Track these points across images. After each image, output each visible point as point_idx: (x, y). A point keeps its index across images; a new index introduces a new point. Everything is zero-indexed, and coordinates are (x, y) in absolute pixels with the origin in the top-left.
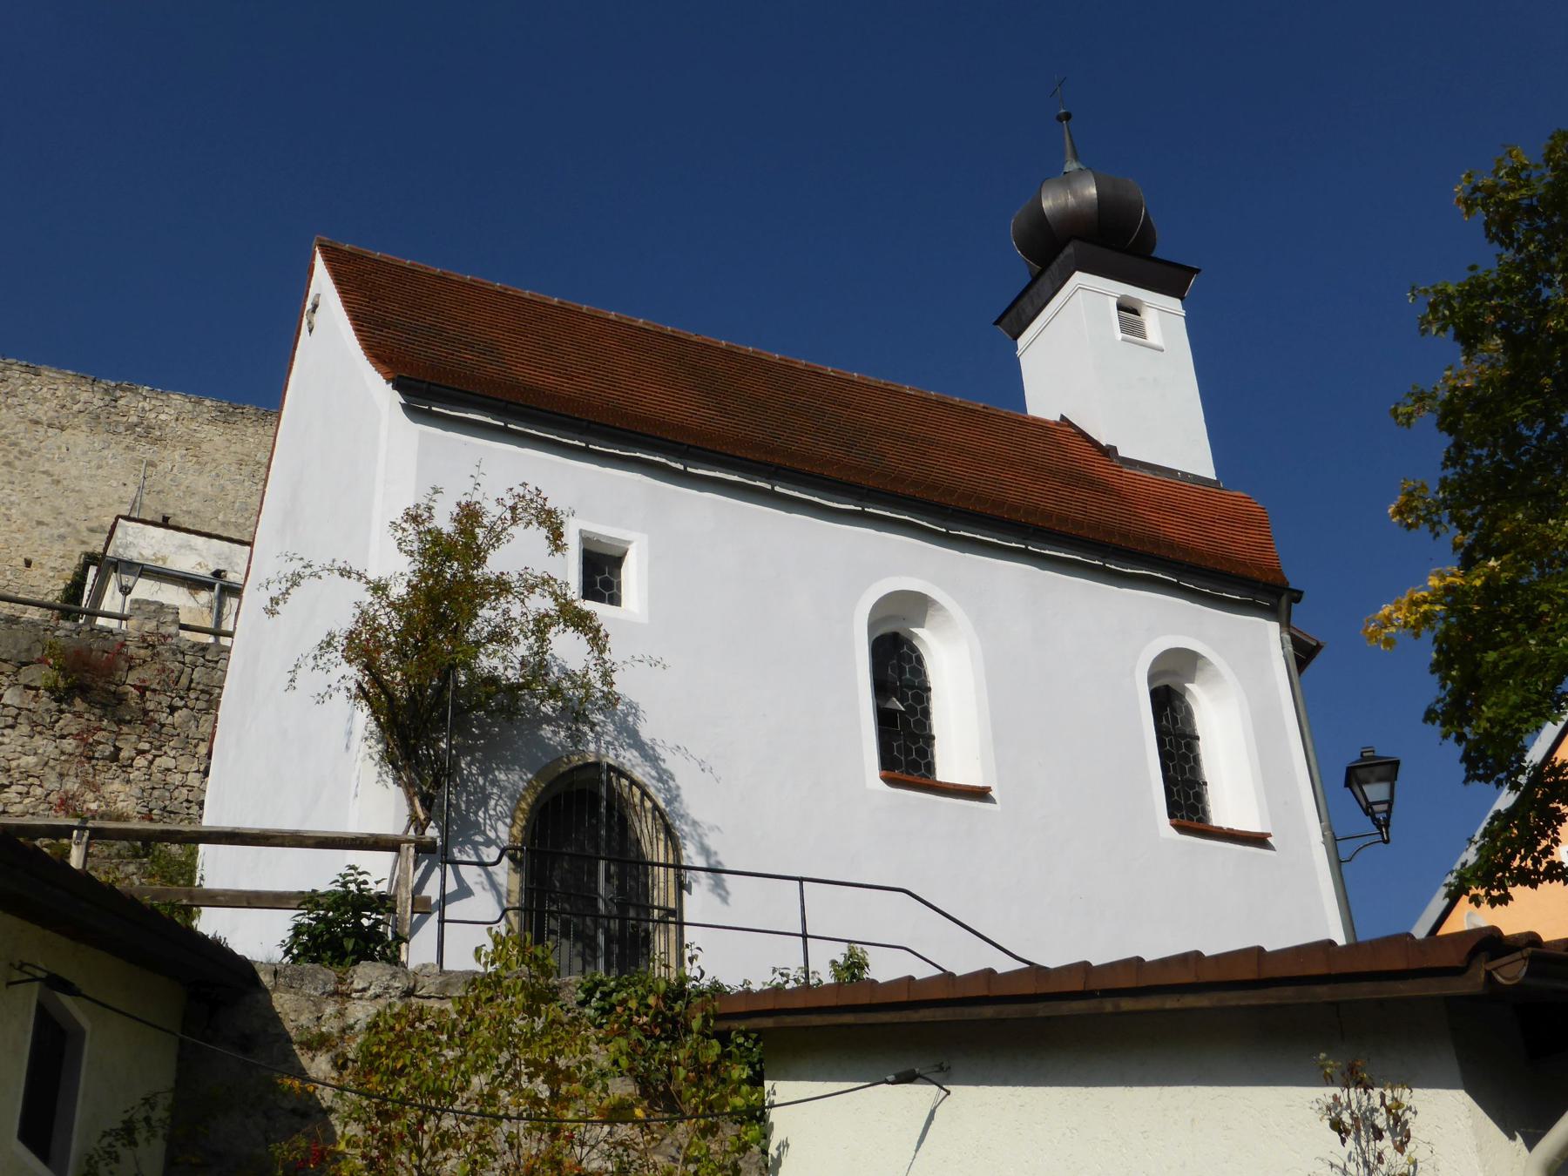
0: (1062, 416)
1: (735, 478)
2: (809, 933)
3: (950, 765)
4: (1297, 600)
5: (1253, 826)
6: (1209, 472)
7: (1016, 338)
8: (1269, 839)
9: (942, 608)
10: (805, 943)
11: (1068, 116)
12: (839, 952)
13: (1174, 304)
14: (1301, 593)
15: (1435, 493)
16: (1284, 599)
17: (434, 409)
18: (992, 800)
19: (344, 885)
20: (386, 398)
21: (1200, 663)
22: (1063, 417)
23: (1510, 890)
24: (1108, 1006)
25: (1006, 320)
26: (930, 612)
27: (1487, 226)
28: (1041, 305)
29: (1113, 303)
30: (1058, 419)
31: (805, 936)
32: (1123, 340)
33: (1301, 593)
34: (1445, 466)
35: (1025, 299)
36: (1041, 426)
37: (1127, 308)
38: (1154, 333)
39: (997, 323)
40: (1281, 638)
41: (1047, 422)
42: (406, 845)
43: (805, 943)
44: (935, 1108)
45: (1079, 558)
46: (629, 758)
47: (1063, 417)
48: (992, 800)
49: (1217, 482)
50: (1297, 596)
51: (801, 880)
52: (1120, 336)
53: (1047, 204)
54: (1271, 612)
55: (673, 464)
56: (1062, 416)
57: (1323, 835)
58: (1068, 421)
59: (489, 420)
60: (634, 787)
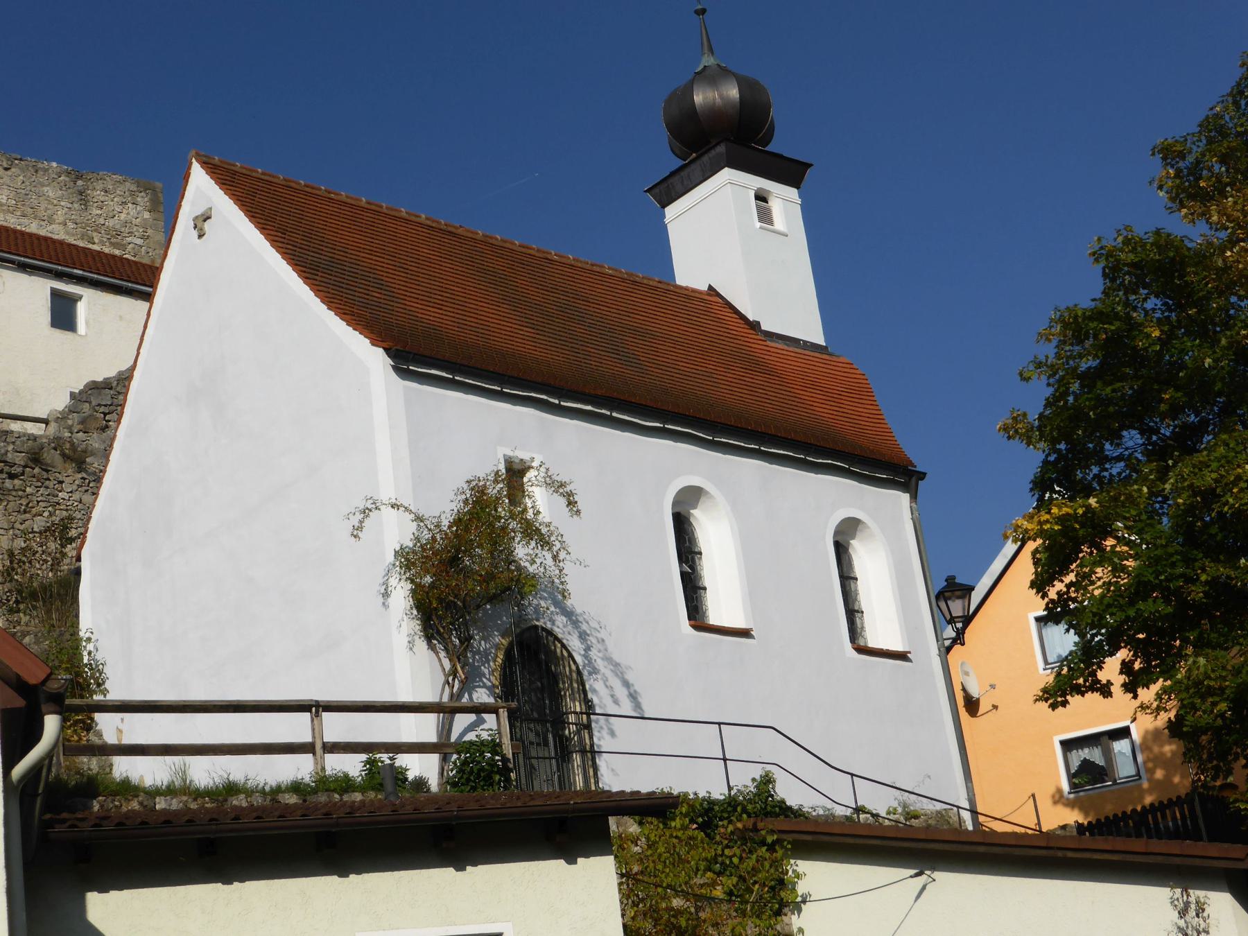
0: (710, 286)
1: (589, 408)
2: (727, 757)
3: (720, 610)
4: (922, 479)
5: (898, 647)
6: (809, 328)
7: (664, 207)
8: (909, 655)
9: (712, 497)
10: (726, 764)
11: (703, 11)
12: (757, 772)
13: (792, 193)
14: (925, 474)
15: (1033, 416)
16: (914, 479)
17: (411, 367)
18: (751, 637)
19: (89, 640)
20: (375, 360)
21: (860, 527)
22: (710, 288)
23: (1069, 697)
24: (1060, 854)
25: (657, 190)
26: (702, 499)
27: (1104, 269)
28: (691, 186)
29: (752, 195)
30: (705, 288)
31: (725, 760)
32: (760, 228)
33: (925, 474)
34: (1046, 406)
35: (676, 179)
36: (689, 295)
37: (761, 197)
38: (779, 223)
39: (648, 191)
40: (911, 507)
41: (694, 291)
42: (502, 710)
43: (726, 764)
44: (926, 884)
45: (791, 454)
46: (560, 626)
47: (710, 288)
48: (751, 637)
49: (826, 348)
50: (922, 476)
51: (719, 724)
52: (758, 225)
53: (698, 98)
54: (904, 487)
55: (552, 400)
56: (710, 286)
57: (939, 650)
58: (714, 290)
59: (444, 374)
60: (556, 642)
